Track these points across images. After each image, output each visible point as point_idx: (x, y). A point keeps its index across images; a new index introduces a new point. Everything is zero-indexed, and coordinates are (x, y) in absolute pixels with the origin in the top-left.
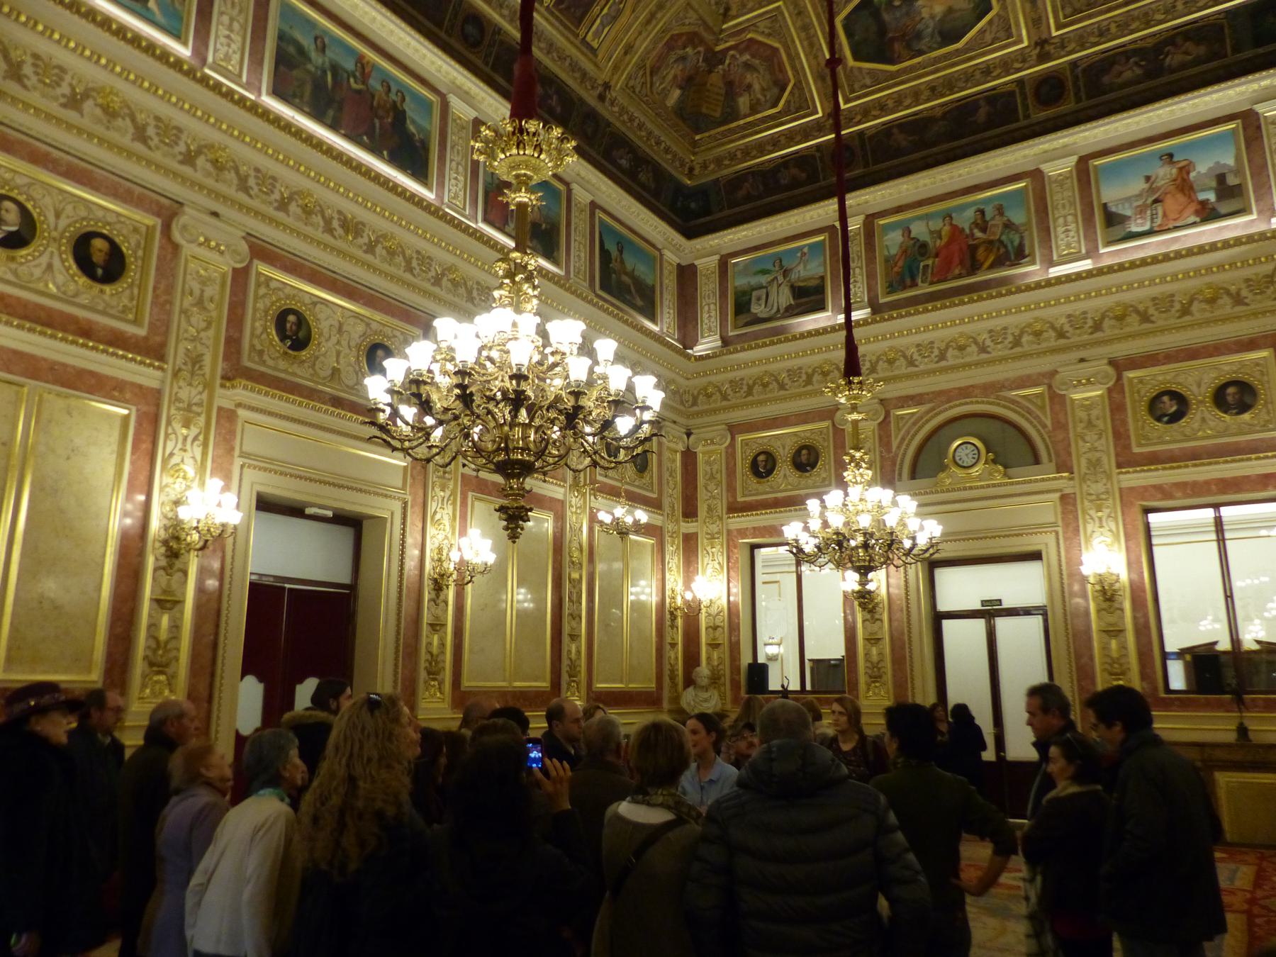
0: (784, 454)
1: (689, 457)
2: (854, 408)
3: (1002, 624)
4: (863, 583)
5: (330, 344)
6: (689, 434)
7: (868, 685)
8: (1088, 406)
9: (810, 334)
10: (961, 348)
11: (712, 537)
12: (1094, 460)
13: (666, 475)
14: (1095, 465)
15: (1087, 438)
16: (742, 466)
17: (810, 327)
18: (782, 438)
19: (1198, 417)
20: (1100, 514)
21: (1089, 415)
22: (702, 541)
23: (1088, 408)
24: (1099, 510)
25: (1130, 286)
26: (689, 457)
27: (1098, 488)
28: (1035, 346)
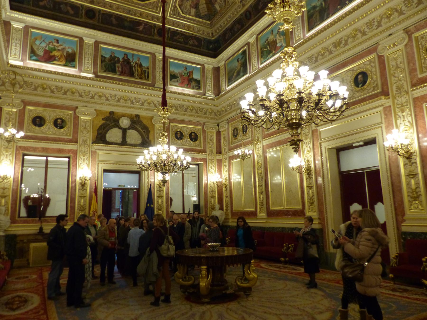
0: (186, 134)
1: (218, 133)
4: (164, 177)
6: (218, 125)
7: (309, 206)
8: (85, 121)
9: (174, 93)
11: (212, 161)
12: (85, 140)
13: (227, 139)
14: (85, 142)
15: (84, 132)
16: (201, 137)
17: (173, 90)
18: (186, 128)
19: (48, 127)
20: (84, 158)
21: (86, 125)
22: (223, 162)
23: (85, 123)
24: (84, 156)
25: (66, 82)
26: (218, 133)
27: (84, 149)
28: (99, 101)
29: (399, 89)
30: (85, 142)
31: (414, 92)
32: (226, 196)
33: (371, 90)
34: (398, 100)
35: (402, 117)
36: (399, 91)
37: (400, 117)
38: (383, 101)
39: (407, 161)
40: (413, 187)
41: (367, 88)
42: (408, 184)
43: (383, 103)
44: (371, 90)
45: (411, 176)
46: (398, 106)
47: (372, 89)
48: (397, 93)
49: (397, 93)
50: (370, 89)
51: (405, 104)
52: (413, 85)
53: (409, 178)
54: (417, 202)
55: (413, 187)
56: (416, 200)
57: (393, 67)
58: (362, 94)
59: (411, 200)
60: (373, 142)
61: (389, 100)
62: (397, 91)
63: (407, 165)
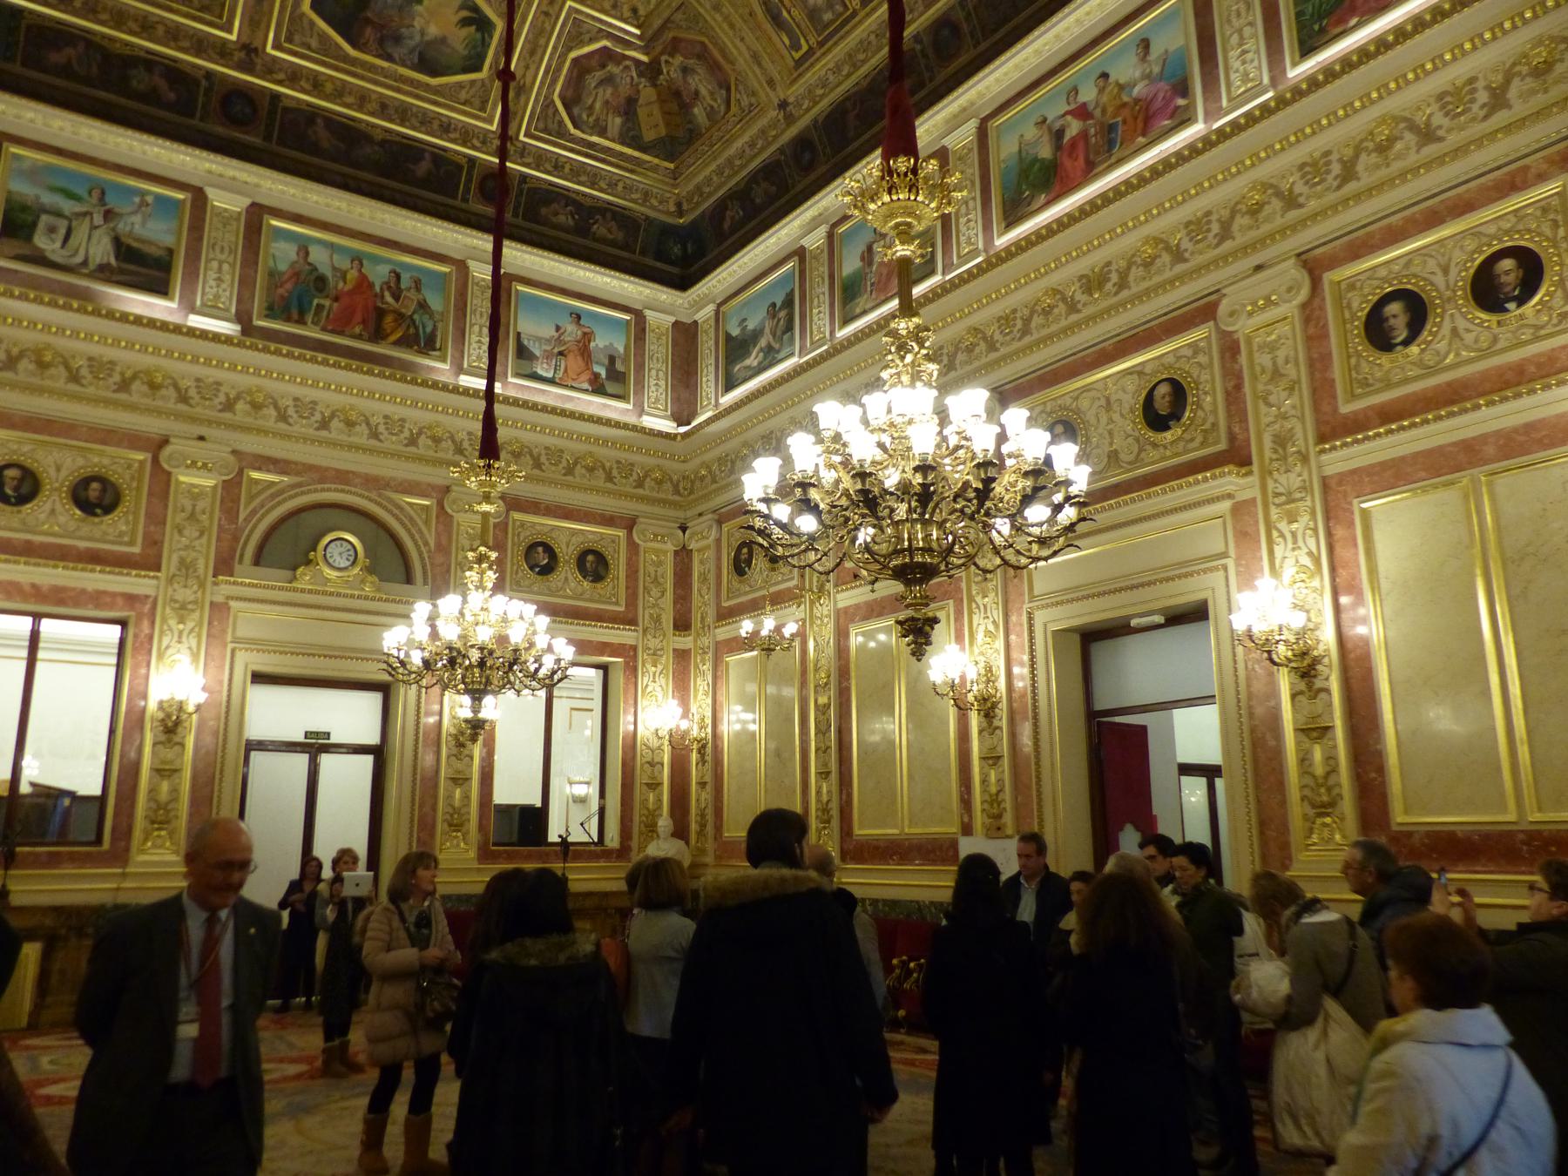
2: (487, 498)
3: (326, 760)
4: (476, 710)
5: (1100, 430)
6: (684, 529)
8: (195, 494)
10: (350, 424)
13: (712, 577)
14: (186, 567)
15: (186, 532)
16: (619, 568)
18: (569, 534)
19: (48, 506)
20: (181, 626)
21: (194, 506)
22: (696, 659)
27: (185, 594)
29: (1281, 441)
30: (186, 567)
31: (1324, 457)
32: (702, 784)
33: (1196, 444)
34: (1276, 481)
35: (1289, 536)
36: (1280, 451)
37: (1282, 535)
38: (1230, 481)
39: (1302, 686)
40: (1319, 770)
41: (1185, 435)
42: (1305, 760)
43: (1230, 488)
44: (1196, 444)
45: (1315, 734)
46: (1277, 501)
47: (1199, 439)
48: (1274, 456)
49: (1274, 456)
50: (1192, 440)
51: (1298, 495)
52: (1322, 438)
53: (1306, 740)
54: (1328, 820)
55: (1319, 770)
56: (1328, 815)
57: (1263, 371)
58: (1168, 453)
59: (1311, 812)
60: (1196, 614)
61: (1249, 479)
62: (1276, 451)
63: (1300, 698)
